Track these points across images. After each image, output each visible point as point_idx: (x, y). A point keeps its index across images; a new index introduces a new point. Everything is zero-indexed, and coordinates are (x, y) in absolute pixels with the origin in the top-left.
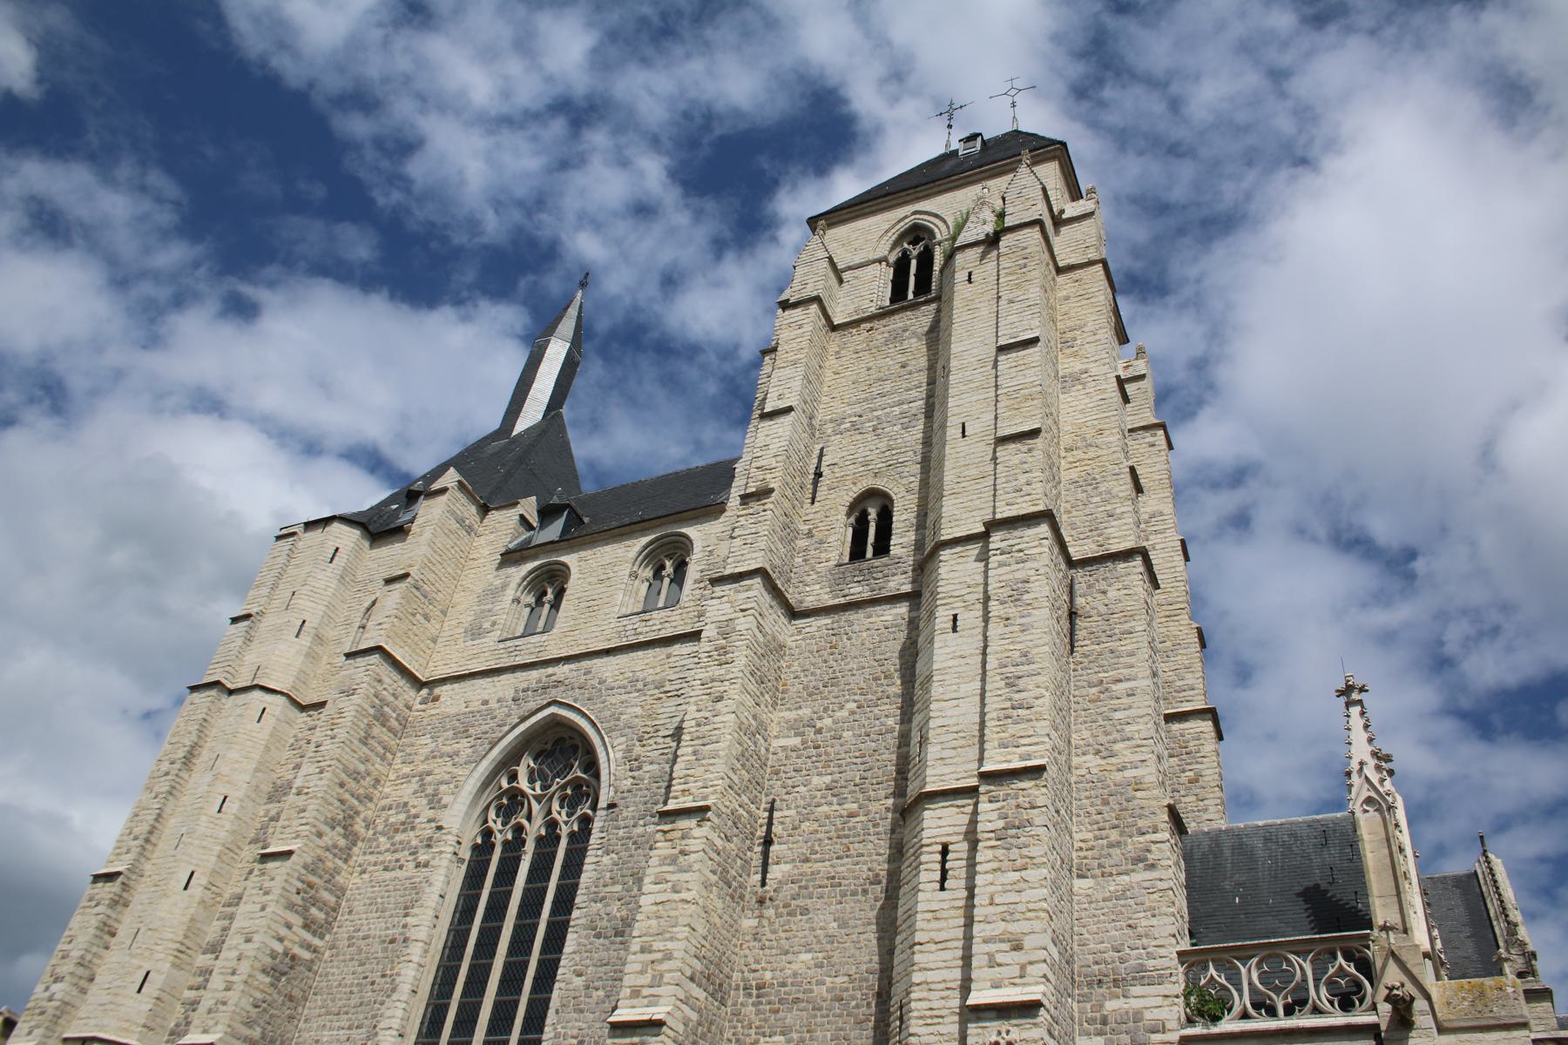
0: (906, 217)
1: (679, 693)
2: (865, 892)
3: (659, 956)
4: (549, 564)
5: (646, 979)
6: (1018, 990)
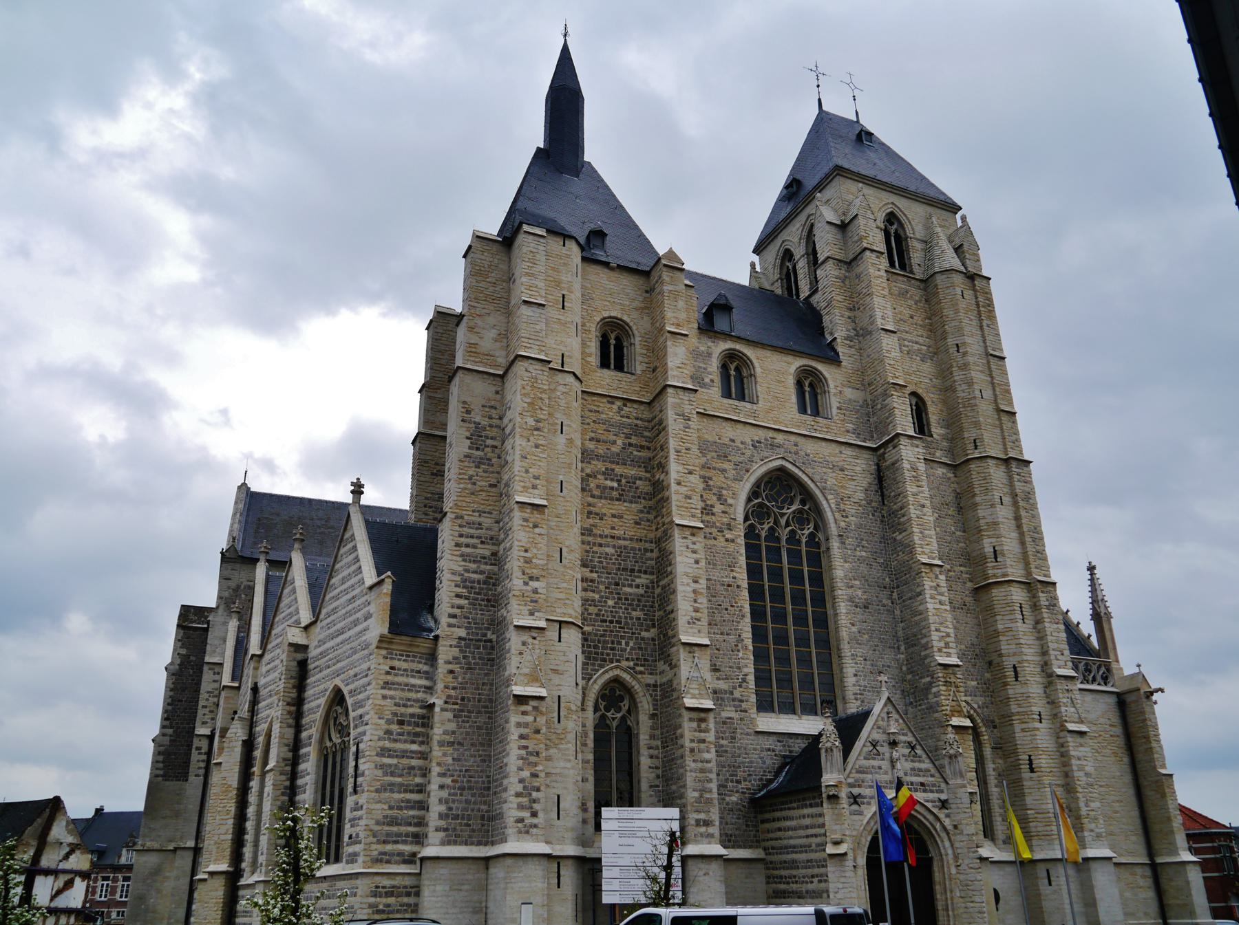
0: (888, 204)
1: (854, 478)
2: (962, 608)
3: (944, 634)
4: (734, 350)
5: (942, 644)
6: (1066, 670)
